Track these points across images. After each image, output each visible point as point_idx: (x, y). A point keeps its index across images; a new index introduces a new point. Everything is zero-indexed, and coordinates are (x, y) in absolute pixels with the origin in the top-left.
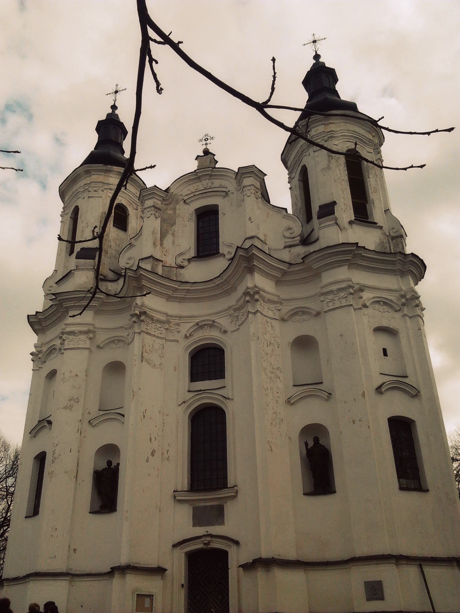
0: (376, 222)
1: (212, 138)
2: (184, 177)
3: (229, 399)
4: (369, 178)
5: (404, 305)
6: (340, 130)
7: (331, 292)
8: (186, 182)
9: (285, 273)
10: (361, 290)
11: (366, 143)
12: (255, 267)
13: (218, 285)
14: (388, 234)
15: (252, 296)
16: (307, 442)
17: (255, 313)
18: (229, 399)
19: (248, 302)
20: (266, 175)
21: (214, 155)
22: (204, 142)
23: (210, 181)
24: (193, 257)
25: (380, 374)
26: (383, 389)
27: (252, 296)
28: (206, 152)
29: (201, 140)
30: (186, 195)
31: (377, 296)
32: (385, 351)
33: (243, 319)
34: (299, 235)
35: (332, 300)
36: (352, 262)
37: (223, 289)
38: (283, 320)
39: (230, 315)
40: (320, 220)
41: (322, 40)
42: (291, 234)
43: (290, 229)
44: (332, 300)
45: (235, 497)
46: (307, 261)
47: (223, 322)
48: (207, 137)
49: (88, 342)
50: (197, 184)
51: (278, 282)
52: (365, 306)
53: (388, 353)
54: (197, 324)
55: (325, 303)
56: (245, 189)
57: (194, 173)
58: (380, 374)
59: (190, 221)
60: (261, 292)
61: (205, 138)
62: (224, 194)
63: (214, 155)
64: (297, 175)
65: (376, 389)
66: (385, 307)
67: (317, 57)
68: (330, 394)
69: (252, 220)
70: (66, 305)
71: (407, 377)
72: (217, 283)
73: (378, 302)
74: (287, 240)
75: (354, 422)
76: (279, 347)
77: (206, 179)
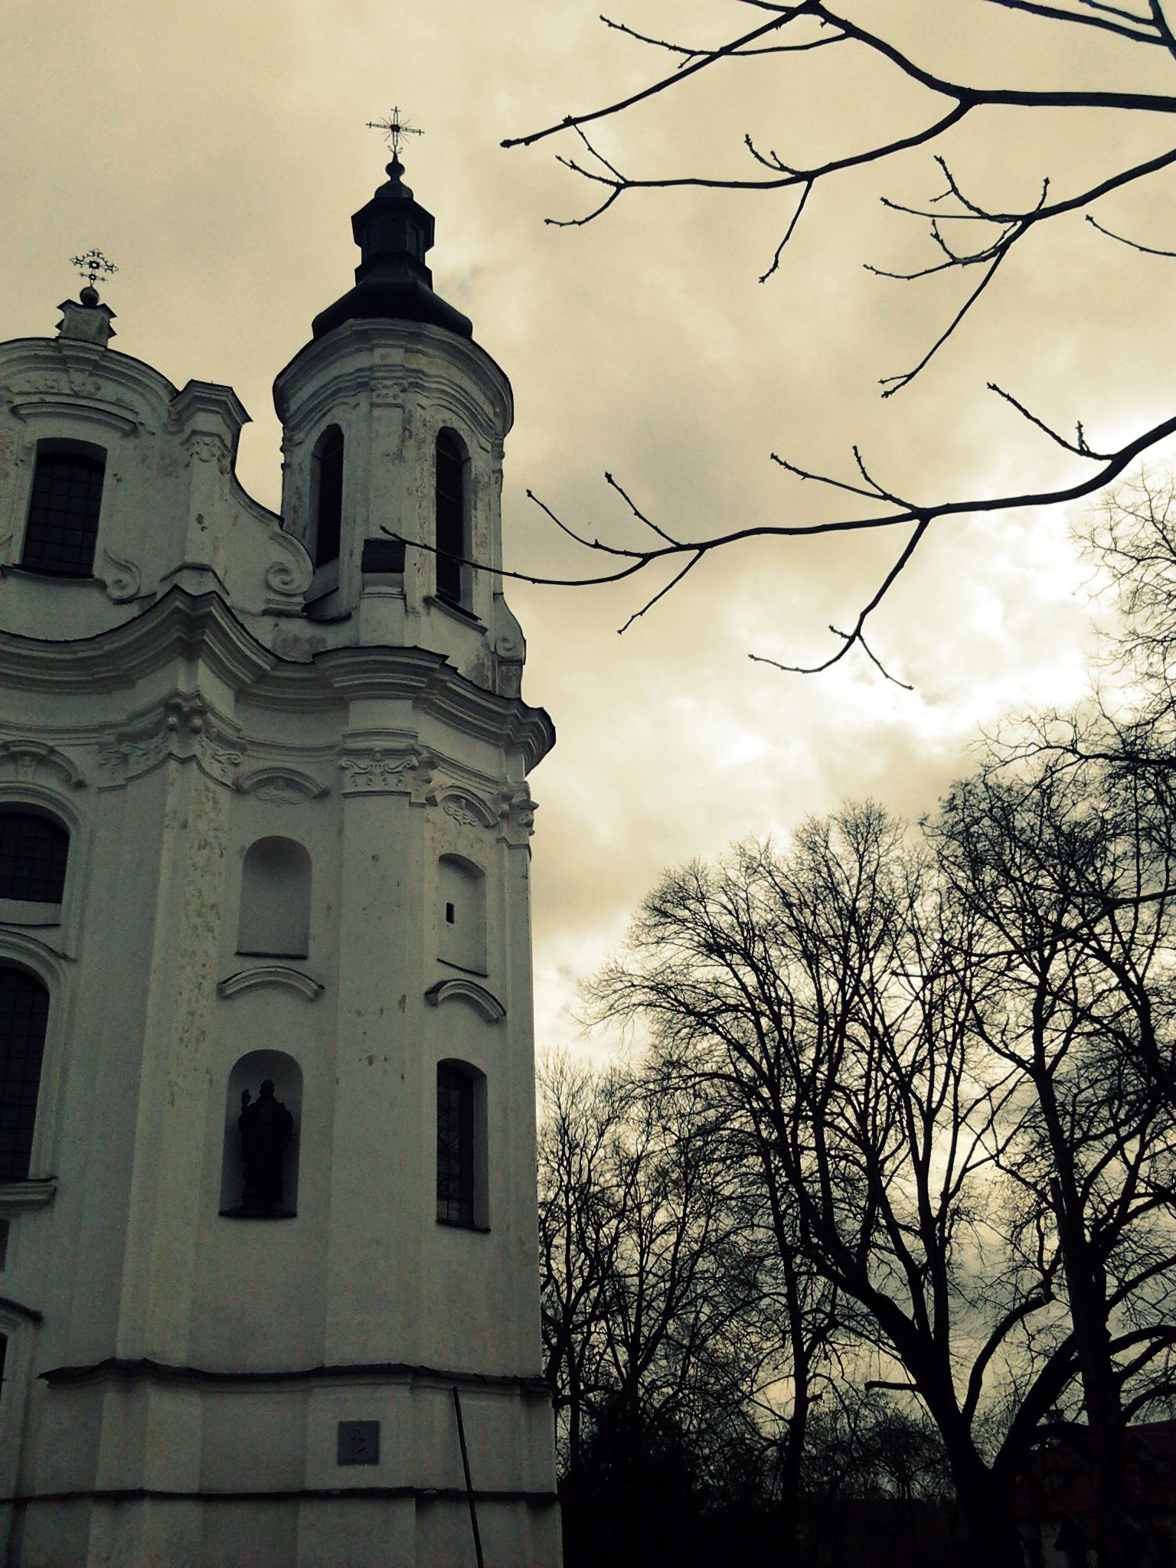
0: (476, 613)
1: (111, 268)
2: (25, 343)
3: (65, 957)
4: (476, 509)
5: (504, 816)
6: (438, 376)
7: (368, 752)
8: (26, 357)
9: (261, 676)
10: (432, 764)
11: (481, 425)
12: (204, 648)
13: (80, 660)
14: (492, 649)
15: (185, 717)
16: (247, 1091)
17: (183, 762)
18: (65, 957)
19: (172, 728)
20: (250, 420)
21: (113, 315)
22: (88, 271)
23: (93, 379)
24: (16, 566)
25: (439, 960)
26: (441, 996)
27: (185, 717)
28: (89, 297)
29: (78, 261)
30: (20, 393)
31: (458, 783)
32: (450, 908)
33: (142, 767)
34: (304, 594)
35: (366, 772)
36: (423, 695)
37: (92, 675)
38: (238, 790)
39: (102, 747)
40: (367, 575)
41: (413, 131)
42: (285, 584)
43: (284, 571)
44: (366, 772)
45: (45, 1205)
46: (323, 665)
47: (80, 757)
48: (95, 258)
50: (55, 375)
51: (242, 695)
52: (431, 801)
53: (456, 917)
55: (348, 774)
56: (198, 438)
57: (52, 344)
58: (439, 960)
59: (20, 464)
60: (210, 716)
61: (92, 259)
62: (127, 427)
63: (113, 315)
64: (310, 439)
65: (427, 993)
66: (467, 813)
67: (395, 168)
68: (322, 987)
69: (206, 523)
71: (485, 976)
72: (80, 655)
73: (456, 799)
74: (272, 596)
75: (371, 1062)
76: (221, 855)
77: (82, 371)
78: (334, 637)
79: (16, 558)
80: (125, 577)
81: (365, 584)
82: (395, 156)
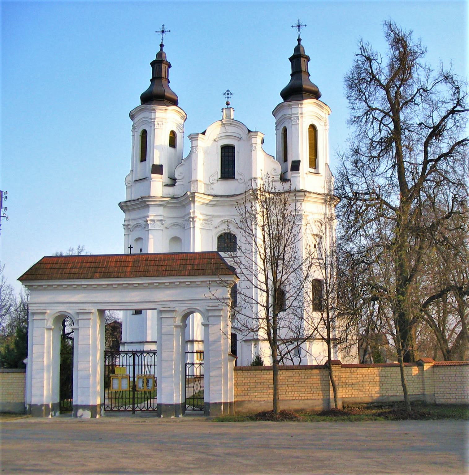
1: (232, 94)
22: (226, 96)
29: (224, 94)
49: (162, 226)
54: (222, 221)
62: (239, 139)
70: (148, 203)
78: (286, 186)
79: (219, 177)
80: (241, 177)
81: (291, 174)
82: (299, 36)
